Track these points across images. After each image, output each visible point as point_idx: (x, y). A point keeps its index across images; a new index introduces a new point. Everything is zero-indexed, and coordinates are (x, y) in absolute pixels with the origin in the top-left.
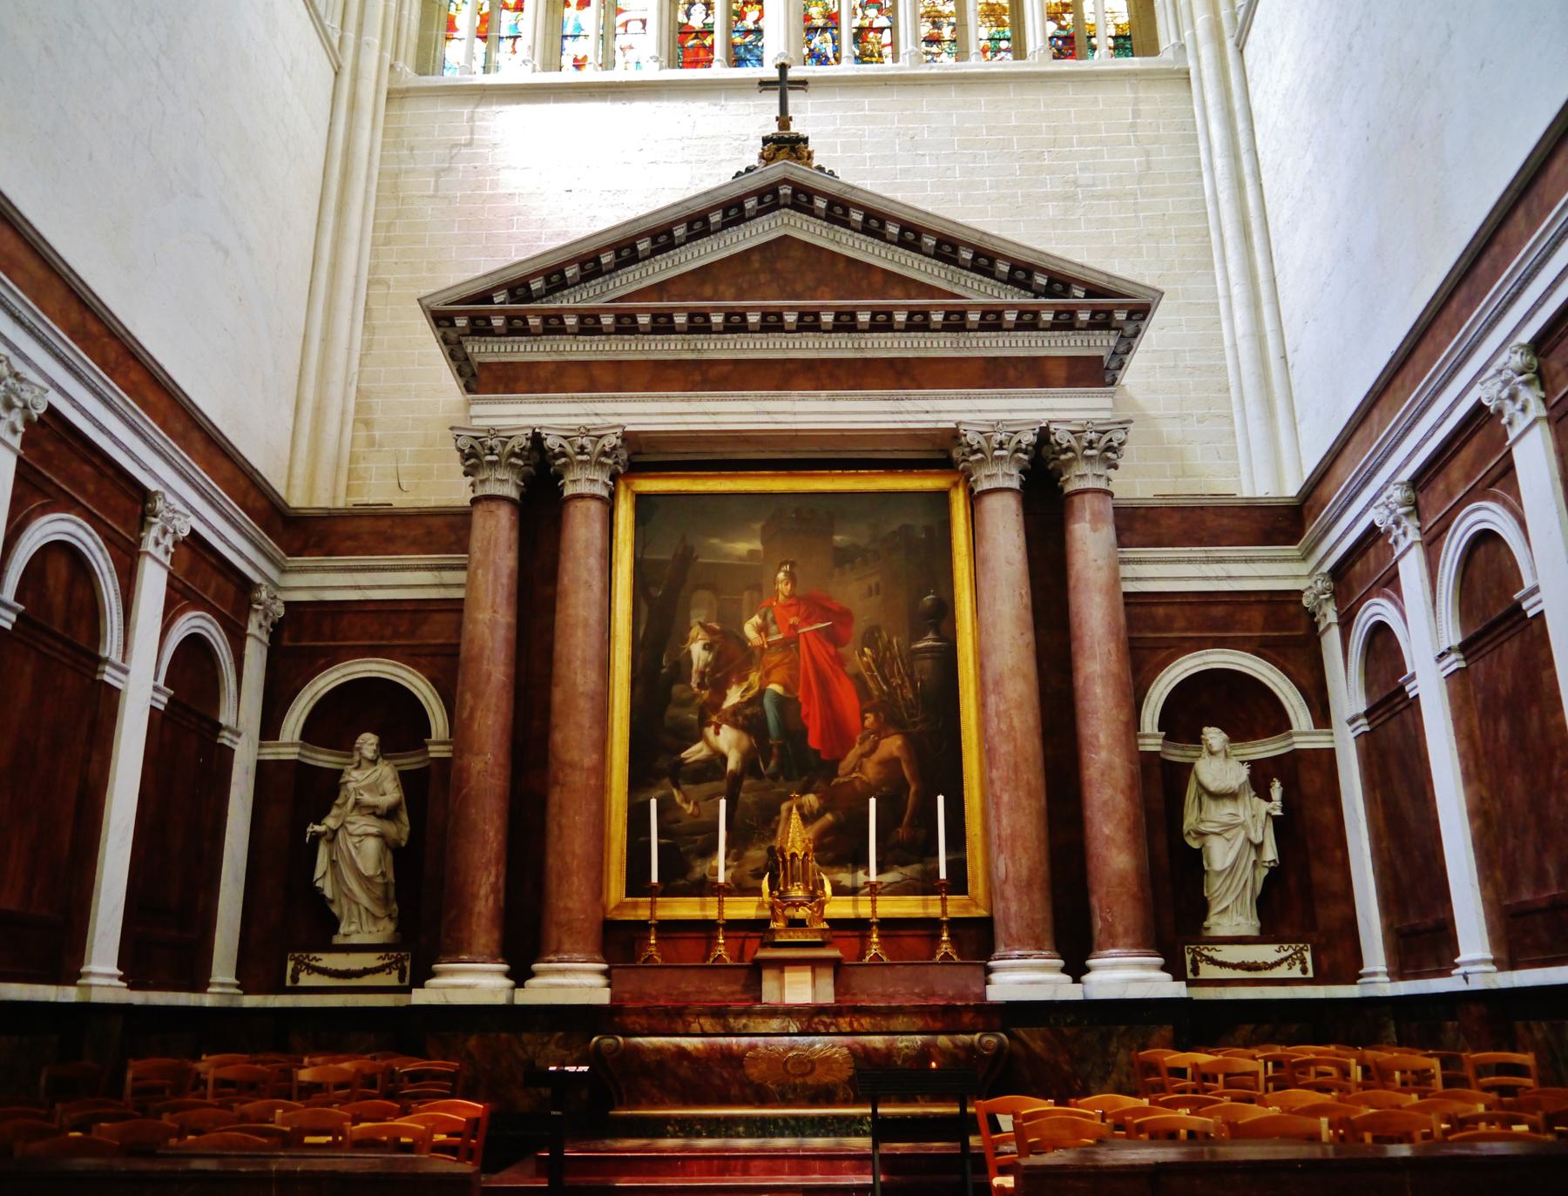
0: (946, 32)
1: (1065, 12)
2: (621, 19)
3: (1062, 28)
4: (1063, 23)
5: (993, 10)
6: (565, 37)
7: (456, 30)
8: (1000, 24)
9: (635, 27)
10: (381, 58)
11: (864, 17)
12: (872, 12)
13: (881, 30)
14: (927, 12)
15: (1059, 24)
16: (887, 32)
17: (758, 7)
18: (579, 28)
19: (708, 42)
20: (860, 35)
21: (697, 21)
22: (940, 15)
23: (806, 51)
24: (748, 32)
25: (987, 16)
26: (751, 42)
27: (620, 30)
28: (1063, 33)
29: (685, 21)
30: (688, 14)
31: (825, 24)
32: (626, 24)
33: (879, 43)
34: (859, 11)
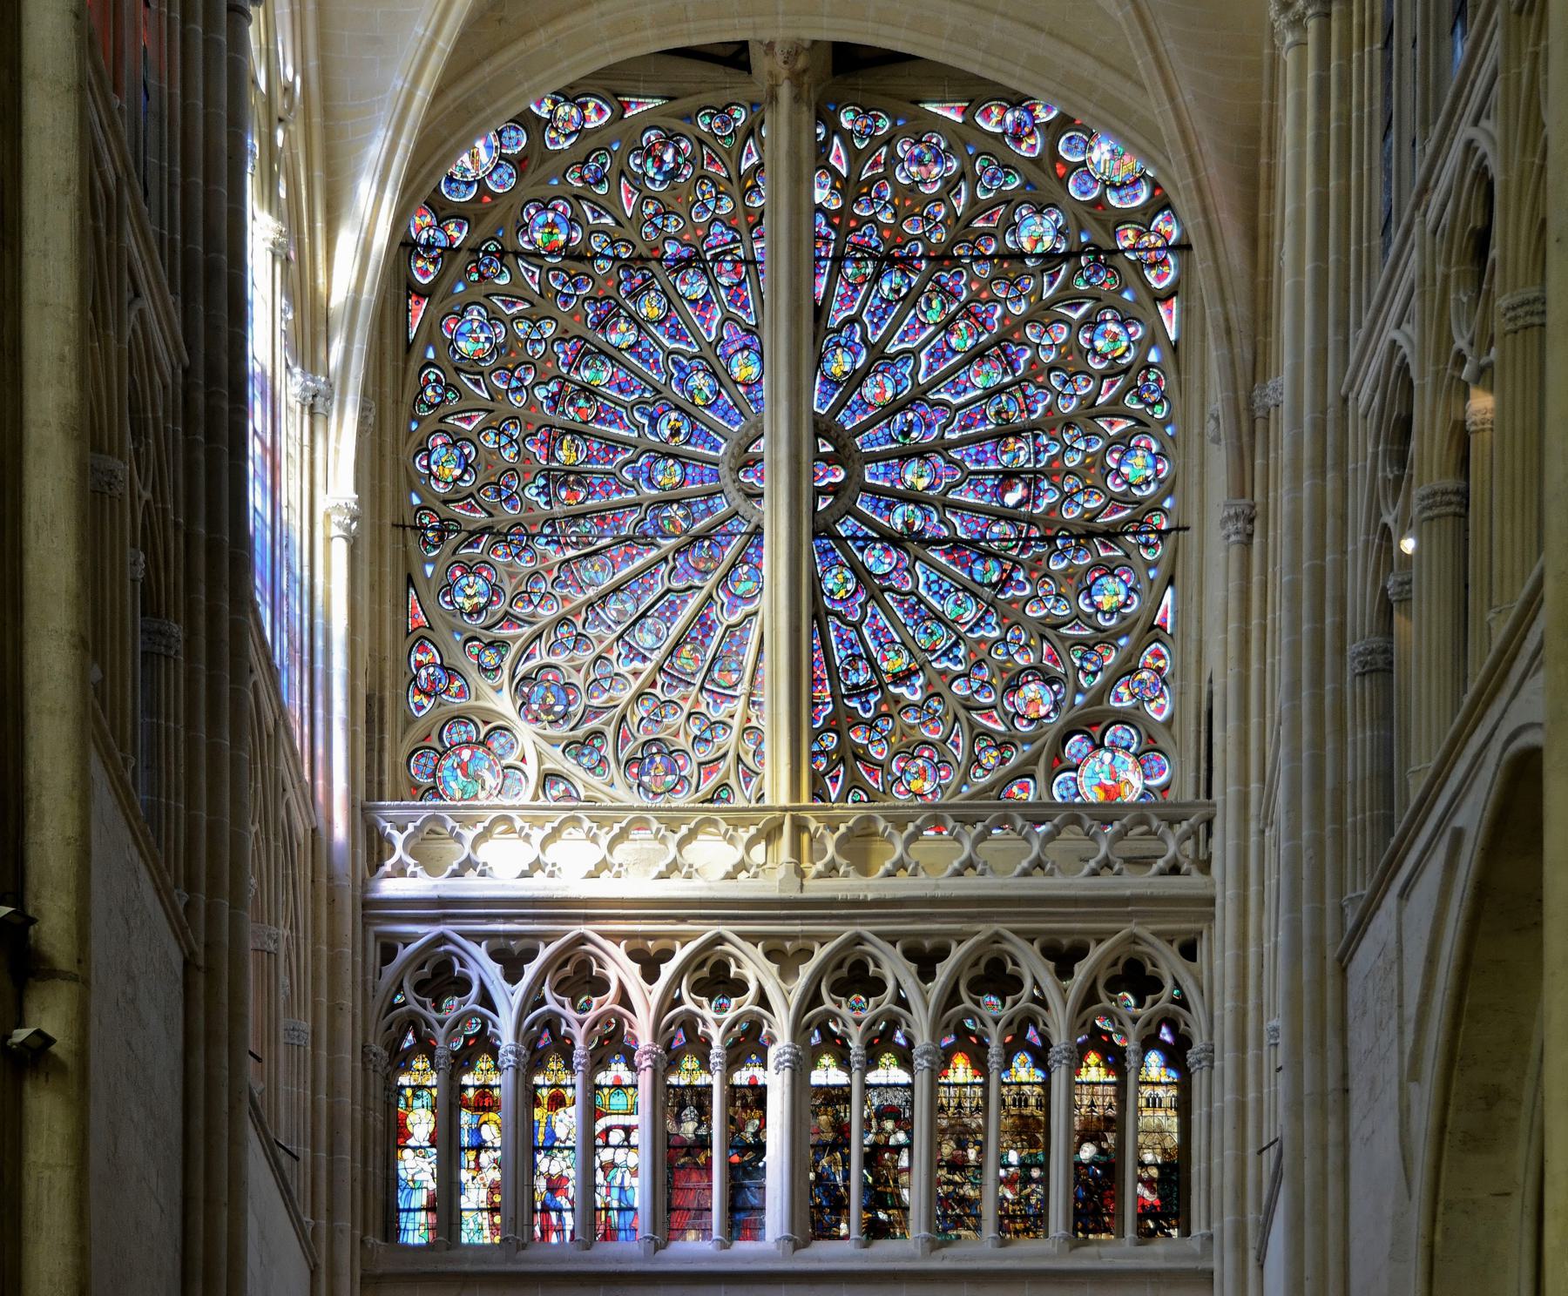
0: (972, 1154)
1: (1107, 1130)
2: (601, 1125)
3: (1101, 1151)
4: (1105, 1146)
5: (1026, 1125)
6: (537, 1149)
7: (410, 1135)
8: (1033, 1143)
9: (616, 1137)
10: (353, 1236)
11: (881, 1130)
12: (889, 1125)
13: (897, 1149)
14: (951, 1126)
15: (1099, 1147)
16: (905, 1154)
17: (759, 1113)
18: (551, 1135)
19: (702, 1160)
20: (872, 1157)
21: (689, 1128)
22: (966, 1129)
23: (812, 1176)
24: (744, 1148)
25: (1019, 1134)
26: (749, 1162)
27: (599, 1142)
28: (1103, 1159)
29: (674, 1131)
30: (679, 1120)
31: (835, 1140)
32: (608, 1130)
33: (895, 1167)
34: (874, 1123)
